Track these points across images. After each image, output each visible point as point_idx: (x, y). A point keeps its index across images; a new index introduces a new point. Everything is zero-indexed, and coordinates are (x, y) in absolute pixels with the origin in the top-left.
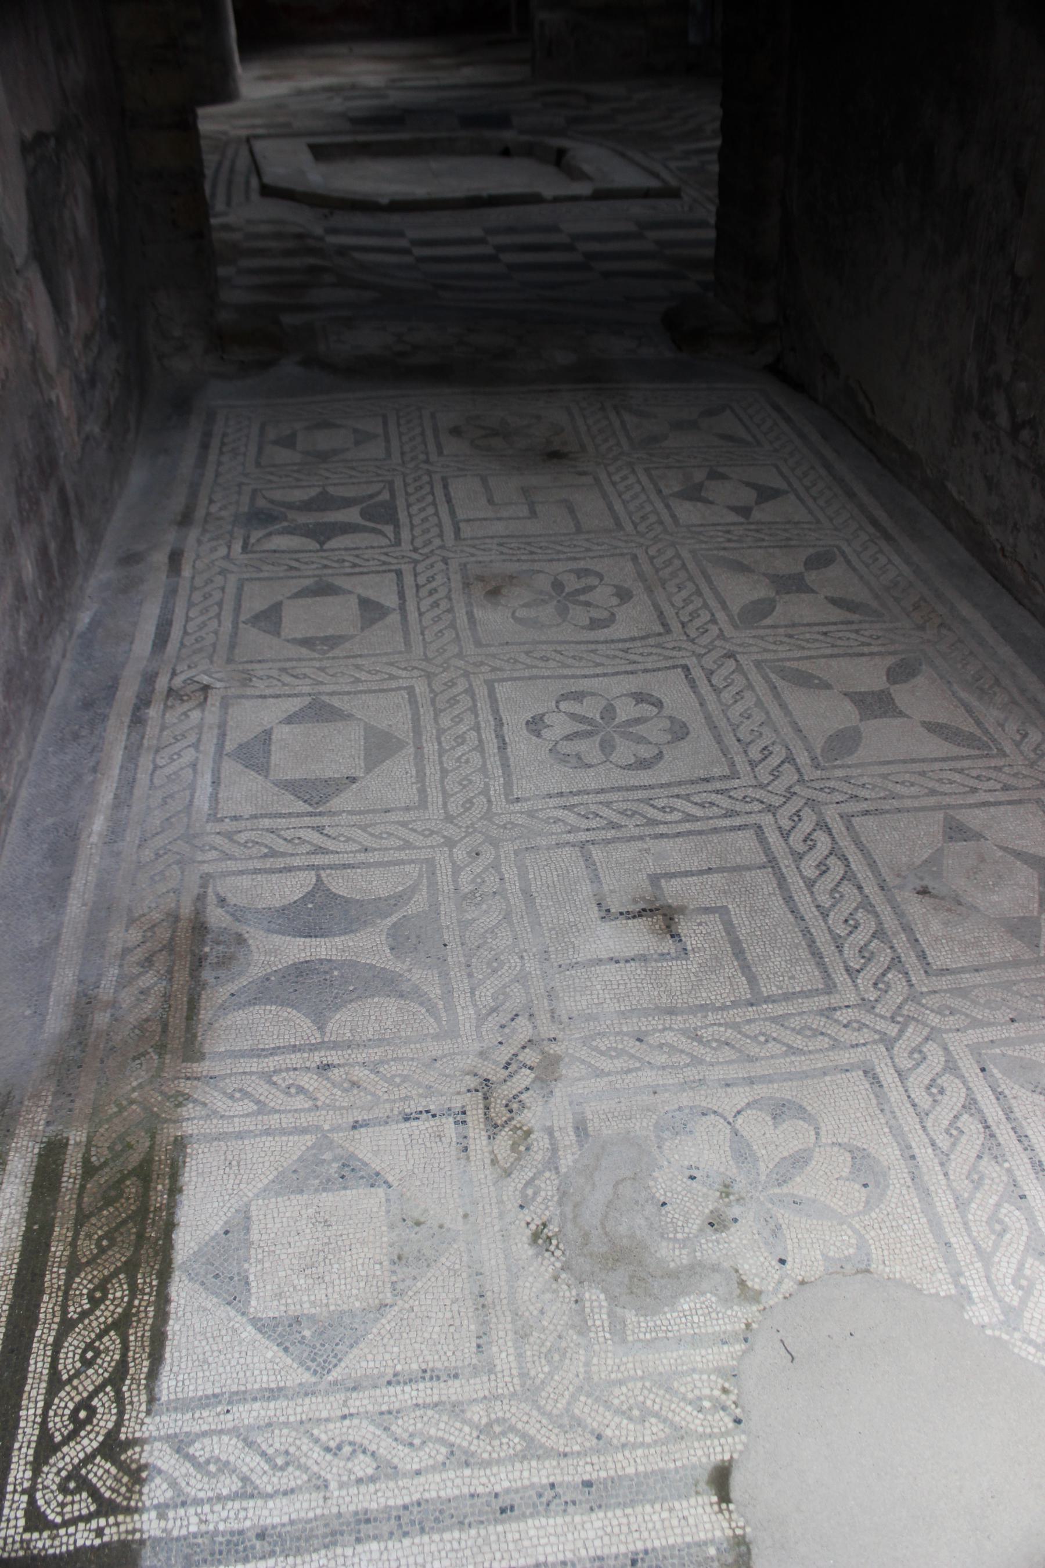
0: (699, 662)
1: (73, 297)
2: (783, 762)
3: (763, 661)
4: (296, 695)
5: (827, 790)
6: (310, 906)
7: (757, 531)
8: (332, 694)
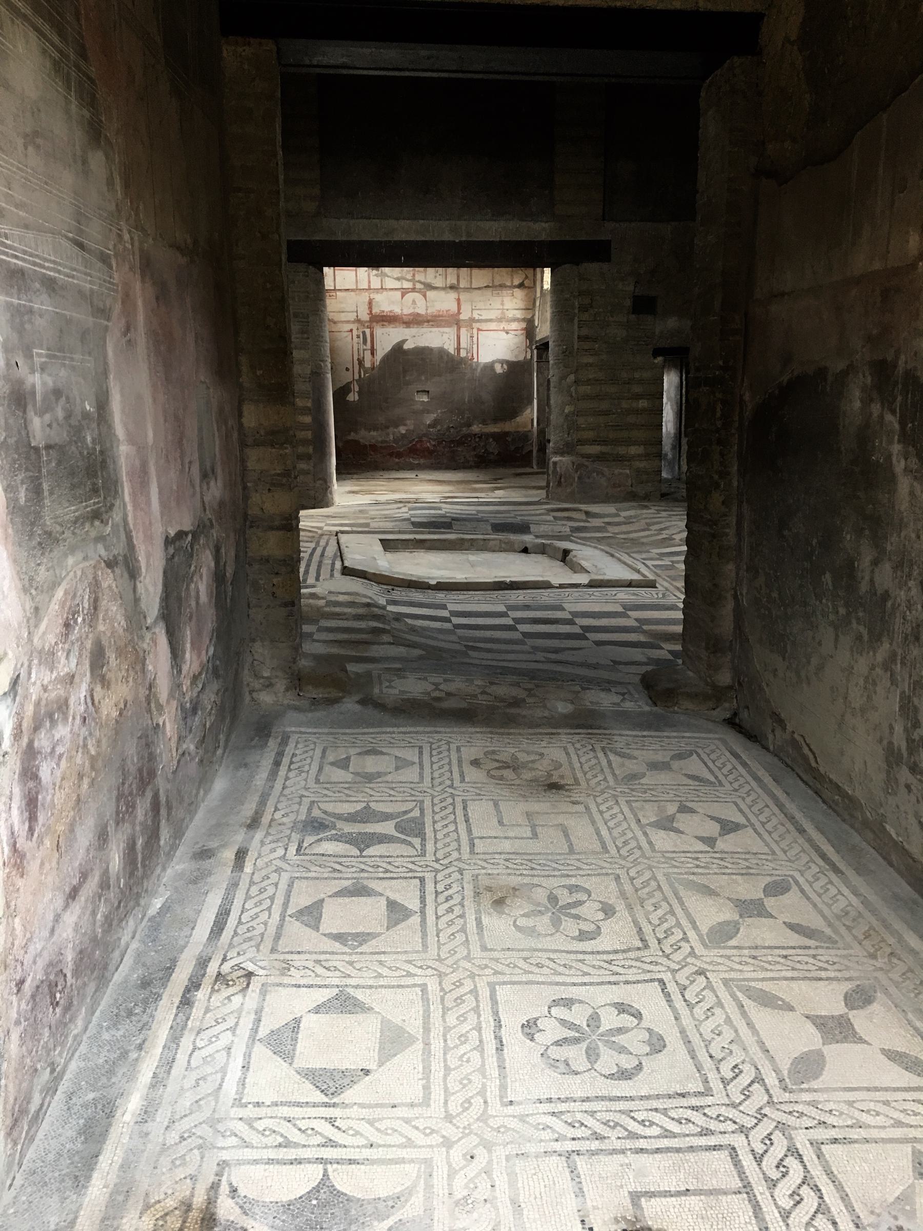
0: (674, 977)
1: (188, 646)
2: (752, 1082)
4: (326, 986)
5: (795, 1114)
6: (314, 1202)
7: (722, 859)
8: (356, 987)
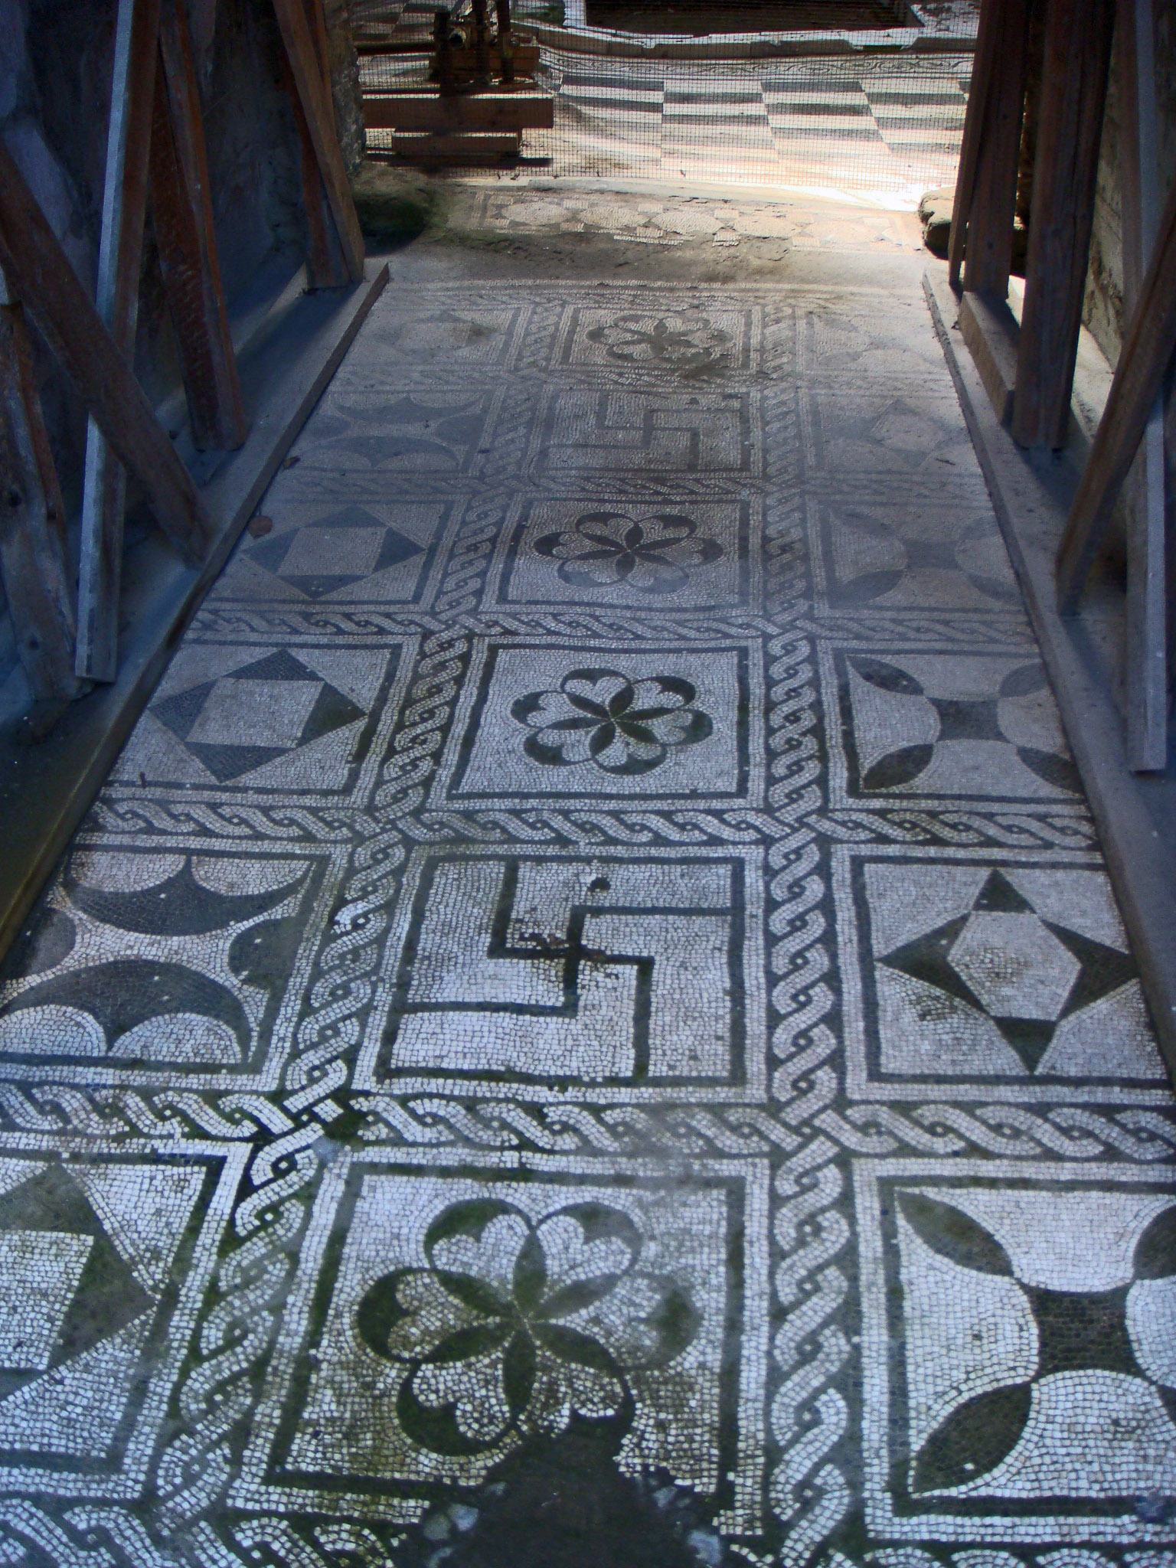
3: (848, 650)
